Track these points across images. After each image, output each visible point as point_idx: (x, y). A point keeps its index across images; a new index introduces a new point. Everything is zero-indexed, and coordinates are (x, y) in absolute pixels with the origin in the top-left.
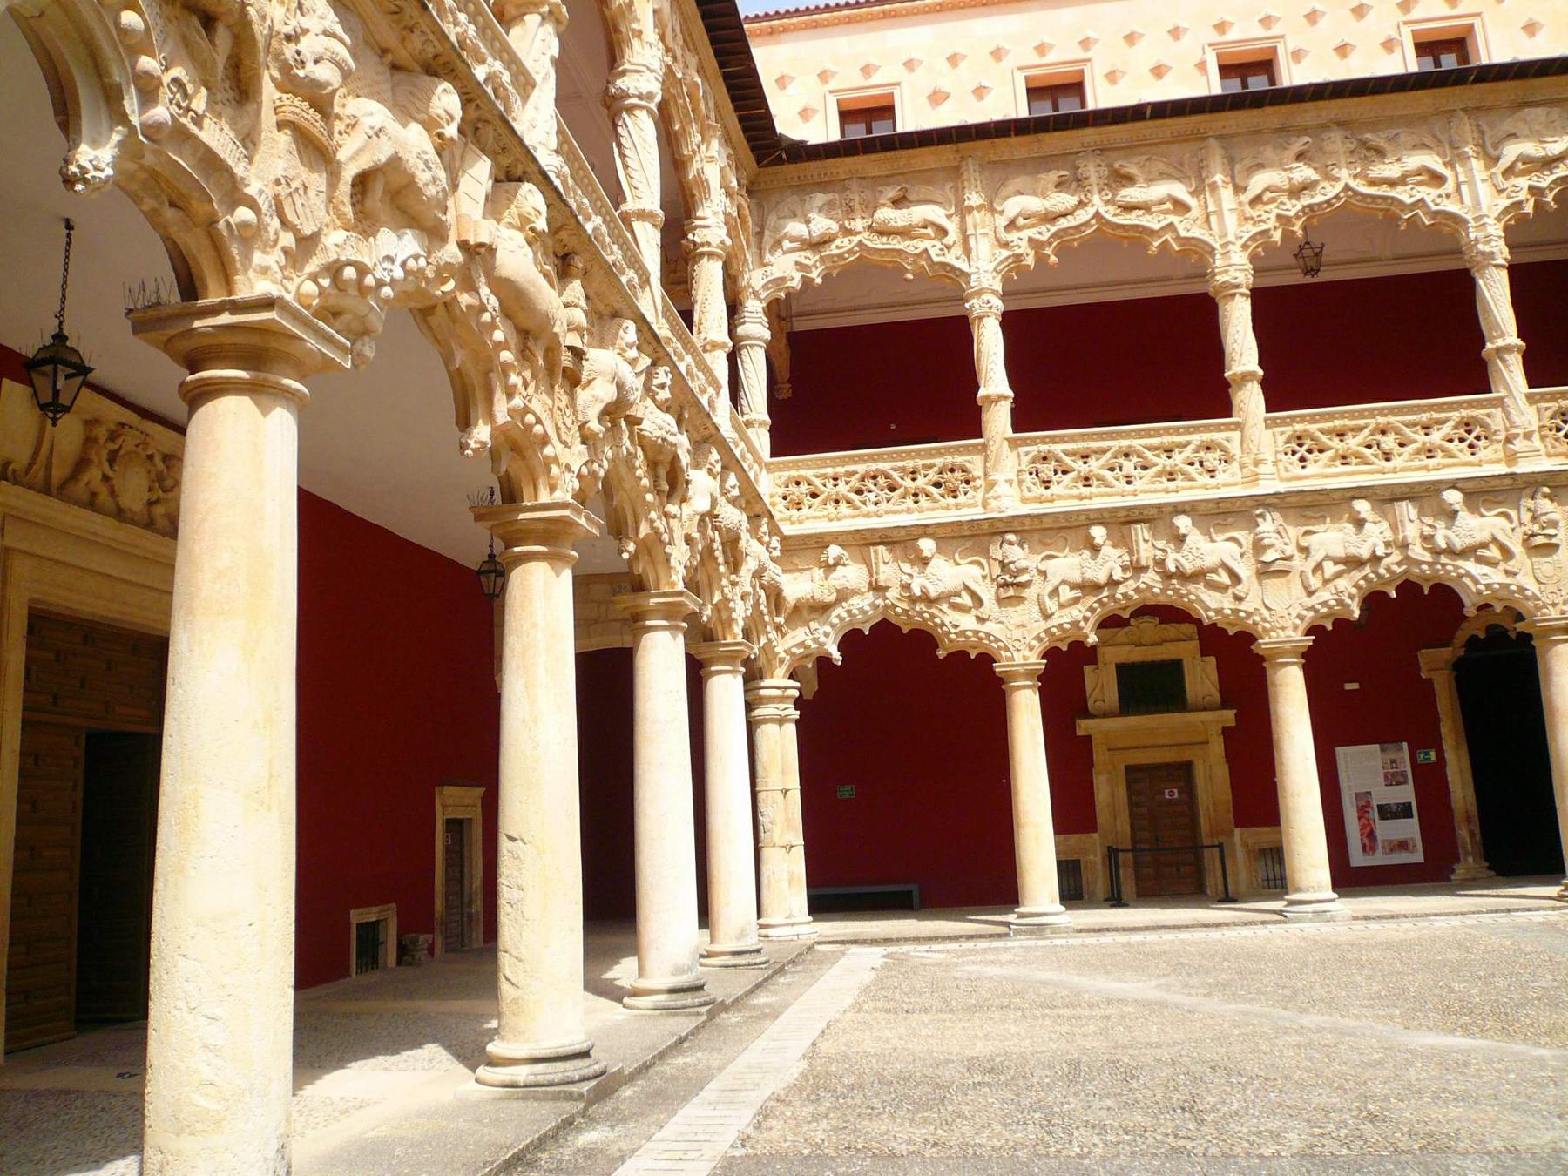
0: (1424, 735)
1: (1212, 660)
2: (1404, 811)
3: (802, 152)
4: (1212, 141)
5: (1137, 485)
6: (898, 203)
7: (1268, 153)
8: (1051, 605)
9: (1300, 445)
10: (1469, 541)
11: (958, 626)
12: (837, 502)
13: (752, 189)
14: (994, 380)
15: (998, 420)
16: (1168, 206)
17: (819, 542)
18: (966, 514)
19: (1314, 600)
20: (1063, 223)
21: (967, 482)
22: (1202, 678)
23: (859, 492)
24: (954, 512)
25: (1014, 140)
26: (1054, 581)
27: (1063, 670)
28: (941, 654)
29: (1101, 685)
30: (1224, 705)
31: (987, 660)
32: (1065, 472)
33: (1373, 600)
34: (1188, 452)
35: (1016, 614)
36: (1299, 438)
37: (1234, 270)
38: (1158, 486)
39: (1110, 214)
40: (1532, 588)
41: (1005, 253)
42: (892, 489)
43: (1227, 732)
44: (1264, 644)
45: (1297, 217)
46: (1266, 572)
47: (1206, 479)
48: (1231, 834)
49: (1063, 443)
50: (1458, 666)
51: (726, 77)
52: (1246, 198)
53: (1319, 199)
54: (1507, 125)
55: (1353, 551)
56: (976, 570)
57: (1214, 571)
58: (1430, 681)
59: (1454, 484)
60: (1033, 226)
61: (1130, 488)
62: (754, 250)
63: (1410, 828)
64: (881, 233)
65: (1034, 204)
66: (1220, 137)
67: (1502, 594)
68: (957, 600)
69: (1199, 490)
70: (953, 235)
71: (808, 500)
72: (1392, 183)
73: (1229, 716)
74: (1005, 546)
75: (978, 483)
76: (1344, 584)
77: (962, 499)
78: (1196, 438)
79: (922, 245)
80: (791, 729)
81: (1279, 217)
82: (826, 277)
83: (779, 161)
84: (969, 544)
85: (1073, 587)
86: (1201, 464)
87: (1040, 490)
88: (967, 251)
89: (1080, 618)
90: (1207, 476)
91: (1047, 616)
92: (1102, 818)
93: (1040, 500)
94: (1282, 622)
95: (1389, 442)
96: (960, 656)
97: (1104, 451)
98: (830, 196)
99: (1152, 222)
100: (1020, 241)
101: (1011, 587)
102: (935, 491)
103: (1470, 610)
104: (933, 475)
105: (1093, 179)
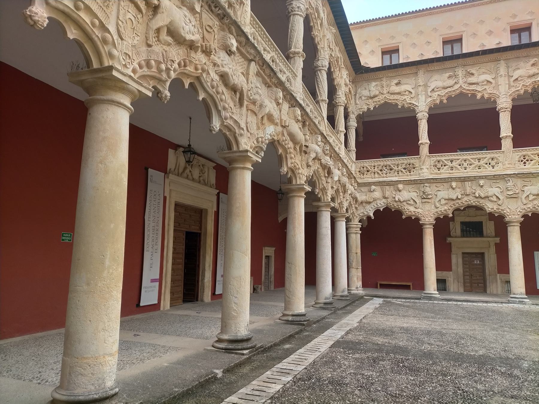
4: (502, 62)
5: (468, 170)
7: (522, 64)
8: (438, 205)
9: (524, 159)
11: (410, 210)
13: (353, 82)
14: (424, 138)
15: (424, 150)
16: (485, 83)
17: (369, 184)
18: (413, 178)
20: (449, 90)
21: (414, 168)
22: (489, 228)
23: (381, 170)
25: (435, 64)
26: (439, 198)
28: (404, 217)
29: (456, 228)
30: (496, 236)
31: (417, 219)
32: (445, 166)
34: (485, 160)
35: (427, 207)
36: (524, 156)
38: (475, 170)
39: (465, 86)
42: (391, 170)
44: (507, 219)
45: (530, 85)
48: (496, 275)
49: (445, 157)
56: (415, 194)
57: (492, 197)
60: (440, 91)
61: (466, 171)
62: (353, 100)
65: (440, 84)
69: (488, 171)
71: (366, 173)
73: (498, 240)
74: (425, 187)
75: (417, 168)
77: (412, 173)
78: (489, 156)
80: (359, 235)
81: (523, 85)
82: (375, 108)
84: (413, 186)
85: (445, 200)
86: (490, 164)
87: (436, 171)
89: (447, 209)
90: (491, 168)
92: (454, 267)
93: (437, 174)
94: (513, 213)
96: (409, 218)
97: (458, 159)
98: (377, 83)
99: (479, 88)
100: (435, 95)
101: (425, 197)
102: (403, 170)
104: (404, 166)
105: (460, 75)
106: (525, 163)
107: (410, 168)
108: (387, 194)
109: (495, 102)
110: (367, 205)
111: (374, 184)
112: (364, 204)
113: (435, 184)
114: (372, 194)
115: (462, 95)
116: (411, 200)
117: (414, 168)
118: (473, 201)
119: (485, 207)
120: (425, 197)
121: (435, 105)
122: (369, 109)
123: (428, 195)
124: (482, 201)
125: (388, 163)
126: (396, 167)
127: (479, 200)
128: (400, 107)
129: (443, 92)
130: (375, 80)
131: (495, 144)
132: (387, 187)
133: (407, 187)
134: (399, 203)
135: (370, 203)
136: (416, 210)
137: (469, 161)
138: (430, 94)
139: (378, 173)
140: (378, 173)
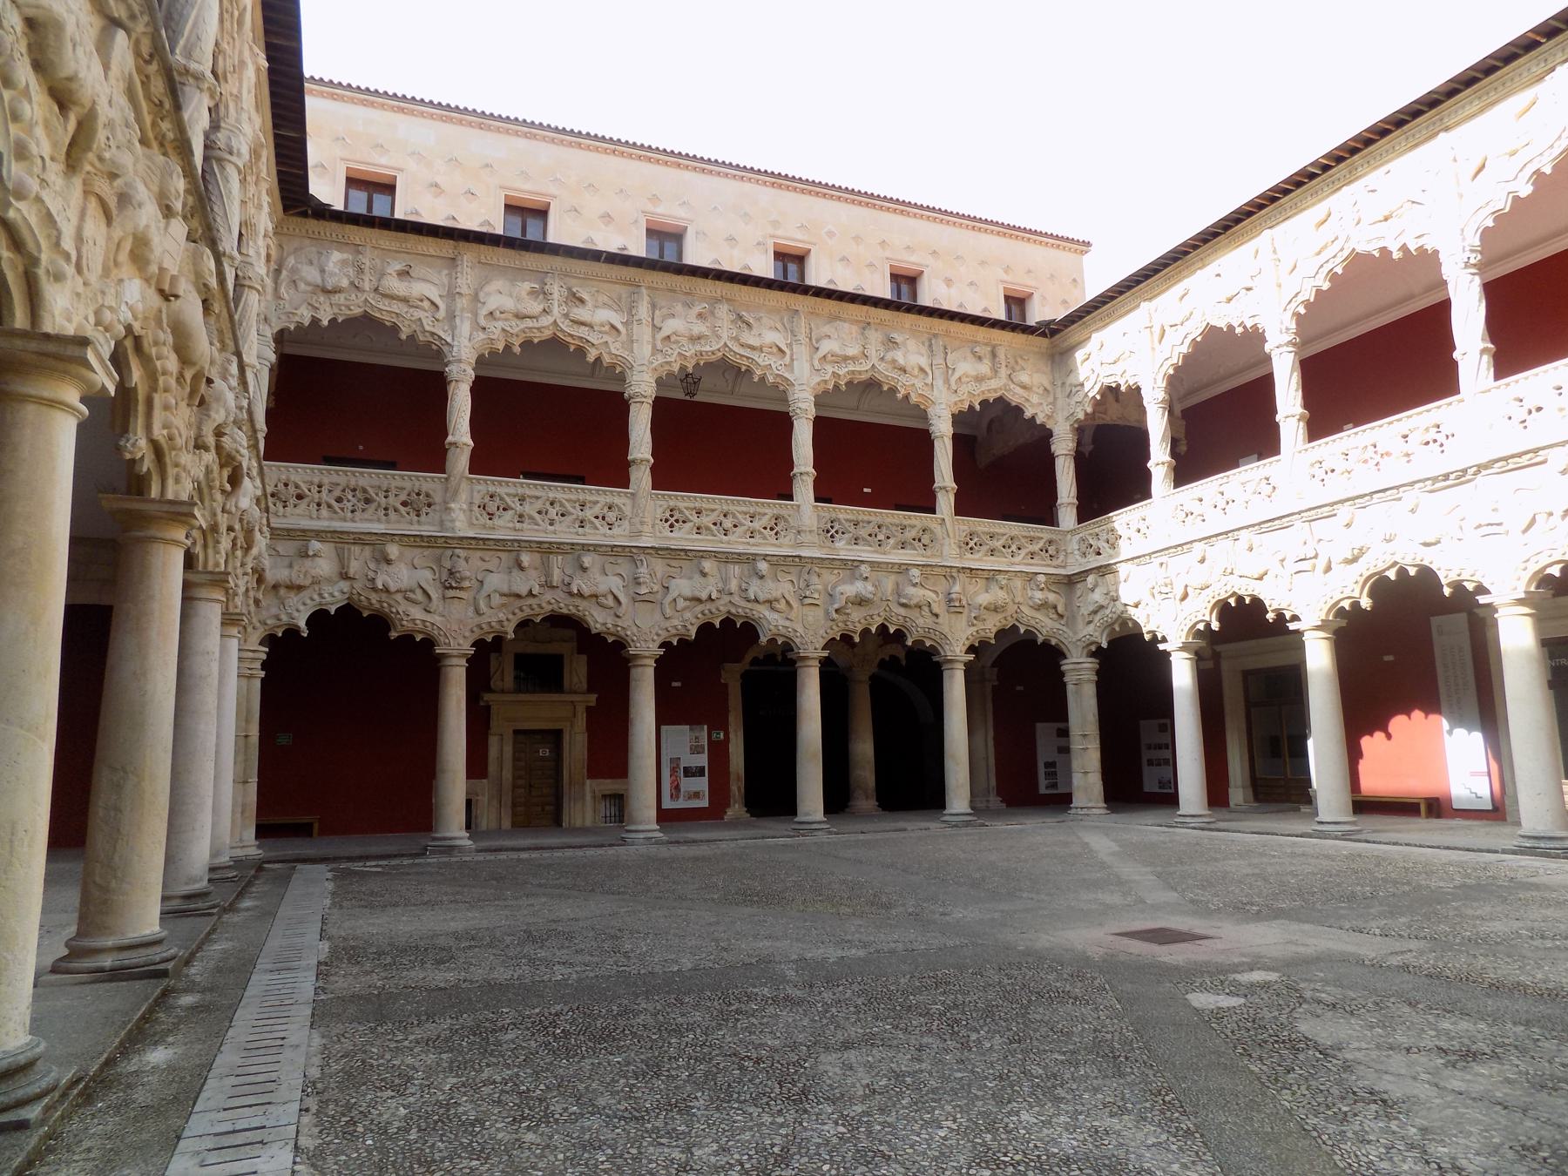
0: (718, 721)
1: (584, 658)
2: (700, 772)
3: (323, 212)
6: (404, 274)
10: (769, 597)
11: (411, 617)
12: (319, 505)
13: (278, 231)
16: (607, 328)
17: (305, 535)
19: (668, 624)
20: (529, 323)
21: (429, 505)
23: (339, 500)
24: (416, 527)
25: (501, 251)
27: (484, 653)
28: (393, 635)
31: (429, 643)
33: (705, 628)
37: (642, 387)
39: (565, 325)
40: (800, 630)
41: (482, 336)
43: (589, 709)
46: (637, 599)
47: (605, 530)
49: (509, 487)
50: (745, 676)
51: (276, 136)
52: (660, 336)
53: (708, 348)
54: (827, 329)
55: (697, 594)
58: (726, 685)
59: (765, 557)
63: (702, 784)
64: (385, 296)
65: (509, 304)
66: (648, 288)
67: (783, 631)
68: (411, 595)
70: (442, 314)
71: (293, 501)
72: (753, 348)
76: (688, 615)
77: (423, 517)
78: (603, 499)
79: (418, 314)
80: (257, 684)
82: (333, 321)
83: (304, 215)
87: (484, 519)
88: (453, 328)
91: (478, 612)
93: (484, 526)
95: (728, 523)
96: (408, 638)
98: (345, 256)
100: (496, 329)
103: (763, 640)
104: (403, 497)
105: (556, 296)
106: (672, 526)
107: (416, 504)
108: (354, 567)
109: (622, 378)
110: (292, 594)
111: (319, 535)
112: (282, 592)
113: (479, 554)
114: (308, 562)
115: (555, 345)
116: (419, 591)
117: (429, 505)
118: (566, 606)
119: (589, 619)
120: (451, 582)
121: (493, 353)
122: (315, 322)
123: (462, 579)
124: (583, 604)
125: (363, 482)
126: (382, 494)
127: (578, 601)
128: (404, 337)
129: (516, 327)
130: (342, 245)
131: (616, 473)
132: (356, 549)
133: (410, 553)
134: (384, 596)
135: (300, 588)
136: (429, 618)
137: (562, 505)
138: (483, 322)
139: (329, 506)
140: (329, 506)
